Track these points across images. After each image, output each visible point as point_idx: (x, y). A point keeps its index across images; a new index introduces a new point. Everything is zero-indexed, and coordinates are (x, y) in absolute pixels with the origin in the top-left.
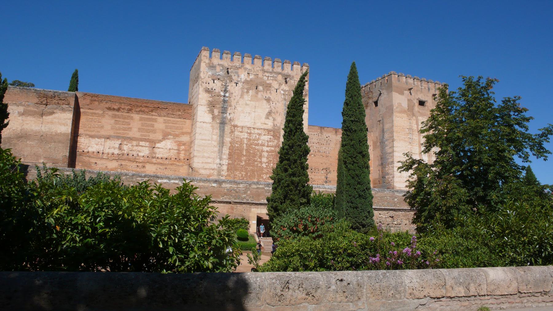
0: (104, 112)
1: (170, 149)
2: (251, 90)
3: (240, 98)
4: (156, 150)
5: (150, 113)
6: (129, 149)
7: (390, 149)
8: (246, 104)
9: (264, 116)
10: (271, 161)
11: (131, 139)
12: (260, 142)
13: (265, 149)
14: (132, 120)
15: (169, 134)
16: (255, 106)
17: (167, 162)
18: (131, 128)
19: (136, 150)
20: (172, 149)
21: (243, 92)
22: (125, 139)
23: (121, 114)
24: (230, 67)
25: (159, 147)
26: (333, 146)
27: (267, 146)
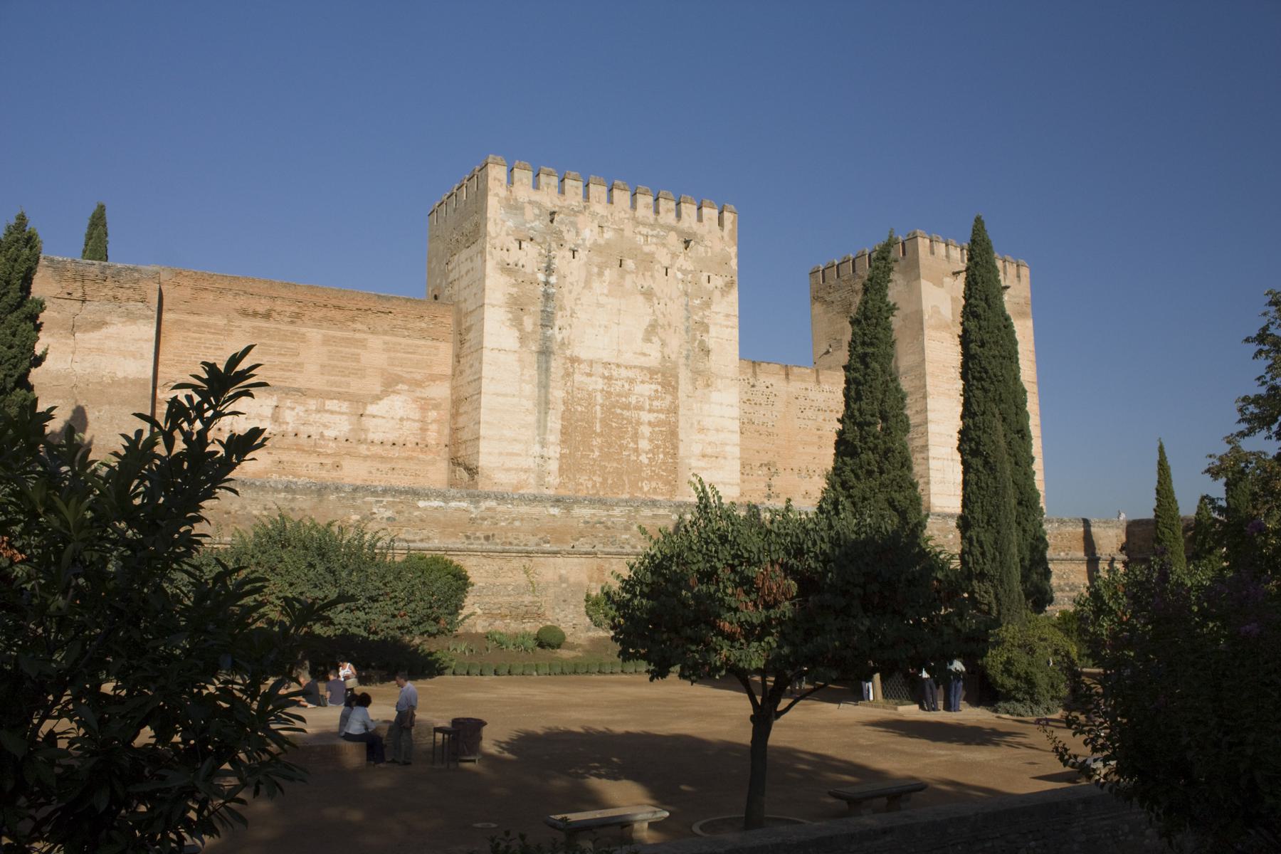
0: (229, 321)
1: (401, 419)
2: (608, 269)
3: (584, 288)
4: (368, 422)
5: (350, 323)
6: (298, 420)
7: (918, 416)
8: (599, 305)
9: (640, 335)
10: (658, 447)
11: (303, 393)
12: (633, 400)
13: (646, 417)
14: (305, 342)
15: (398, 379)
16: (619, 310)
17: (395, 453)
18: (303, 364)
19: (315, 423)
20: (408, 419)
21: (589, 275)
22: (287, 394)
23: (273, 326)
24: (556, 209)
25: (375, 413)
26: (783, 410)
27: (650, 411)
